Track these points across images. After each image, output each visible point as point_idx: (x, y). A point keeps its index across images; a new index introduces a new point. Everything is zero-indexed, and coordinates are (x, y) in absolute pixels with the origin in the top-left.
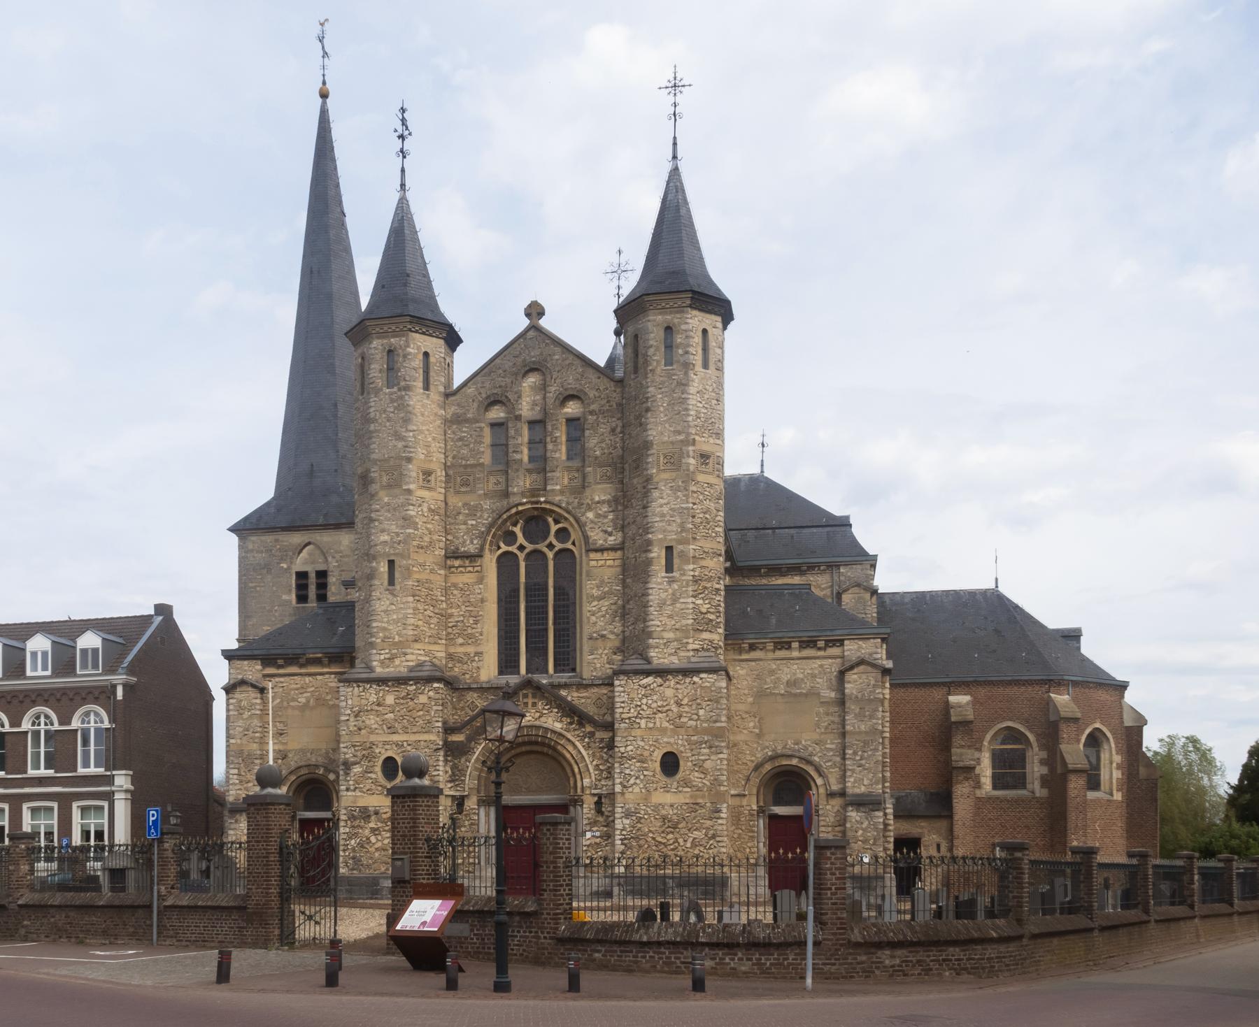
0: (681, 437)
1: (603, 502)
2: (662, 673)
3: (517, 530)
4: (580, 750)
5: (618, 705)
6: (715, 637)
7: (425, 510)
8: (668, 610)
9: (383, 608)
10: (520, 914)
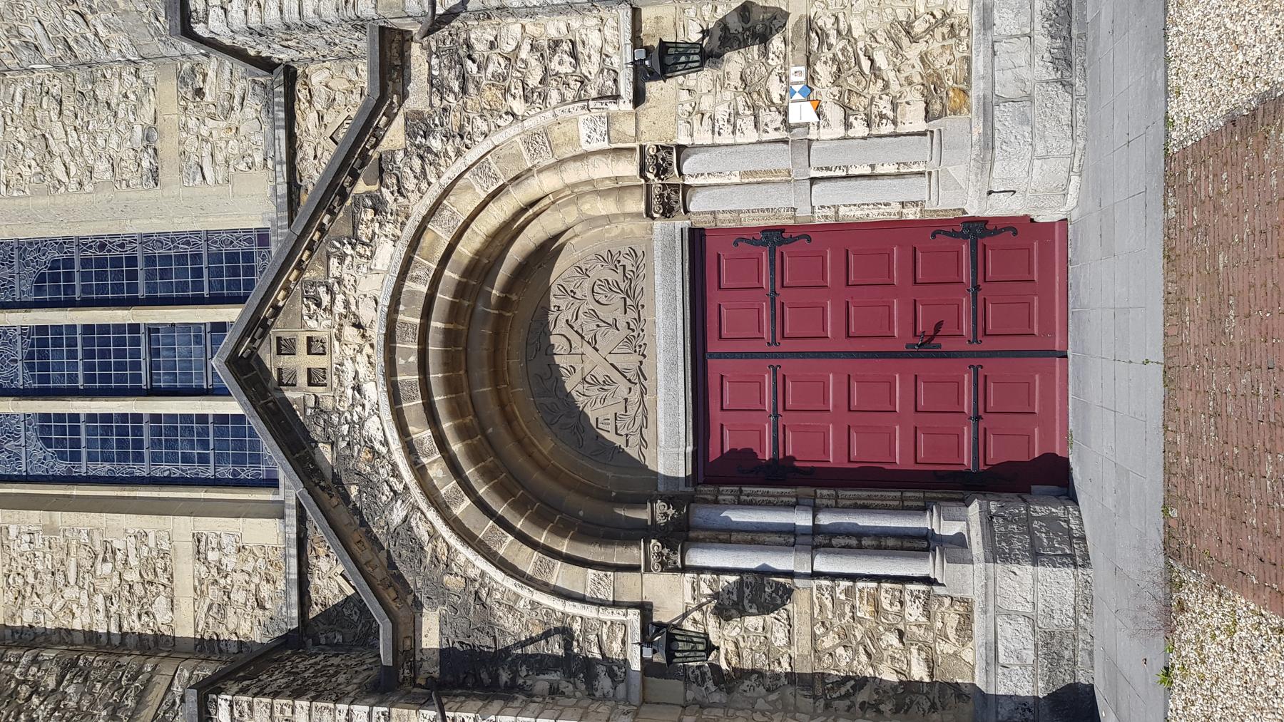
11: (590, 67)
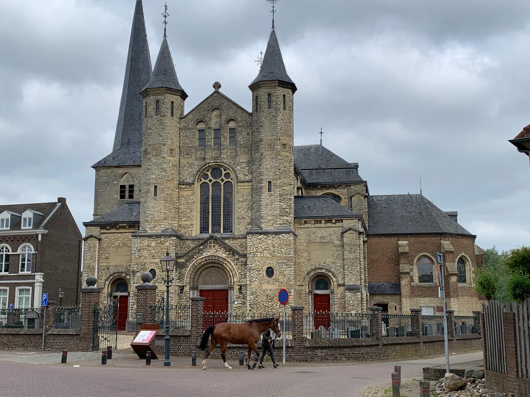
0: (275, 137)
1: (244, 162)
2: (266, 233)
3: (209, 173)
4: (232, 265)
5: (248, 247)
6: (289, 218)
7: (171, 165)
8: (269, 207)
9: (152, 205)
10: (183, 336)
11: (242, 280)
